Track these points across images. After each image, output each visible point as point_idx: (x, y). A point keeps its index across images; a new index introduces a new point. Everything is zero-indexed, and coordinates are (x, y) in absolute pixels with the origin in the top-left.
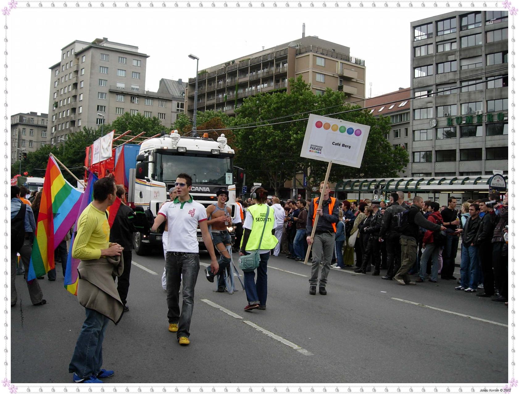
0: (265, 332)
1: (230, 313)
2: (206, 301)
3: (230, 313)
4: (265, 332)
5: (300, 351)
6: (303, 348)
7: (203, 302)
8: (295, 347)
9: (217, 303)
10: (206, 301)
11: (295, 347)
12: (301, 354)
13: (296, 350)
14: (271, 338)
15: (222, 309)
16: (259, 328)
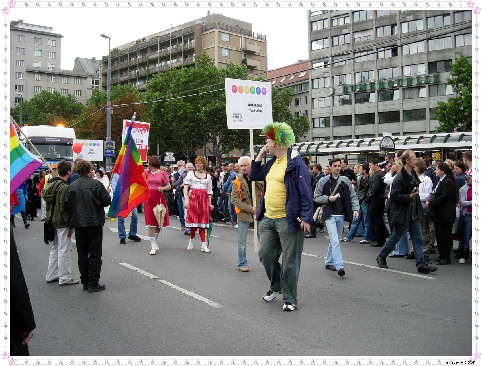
0: (179, 289)
1: (147, 274)
2: (124, 264)
3: (147, 274)
4: (179, 289)
5: (211, 304)
6: (214, 301)
7: (121, 265)
8: (206, 301)
9: (135, 265)
11: (206, 301)
12: (212, 307)
13: (207, 304)
14: (185, 294)
15: (139, 270)
16: (173, 286)
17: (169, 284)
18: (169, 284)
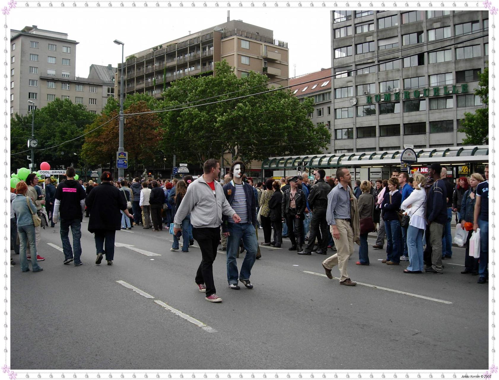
0: (174, 310)
2: (121, 282)
4: (174, 310)
6: (208, 325)
7: (118, 283)
8: (200, 324)
9: (132, 284)
10: (121, 282)
11: (200, 324)
12: (205, 331)
13: (201, 328)
14: (179, 317)
15: (135, 289)
16: (168, 307)
17: (164, 304)
18: (164, 304)
